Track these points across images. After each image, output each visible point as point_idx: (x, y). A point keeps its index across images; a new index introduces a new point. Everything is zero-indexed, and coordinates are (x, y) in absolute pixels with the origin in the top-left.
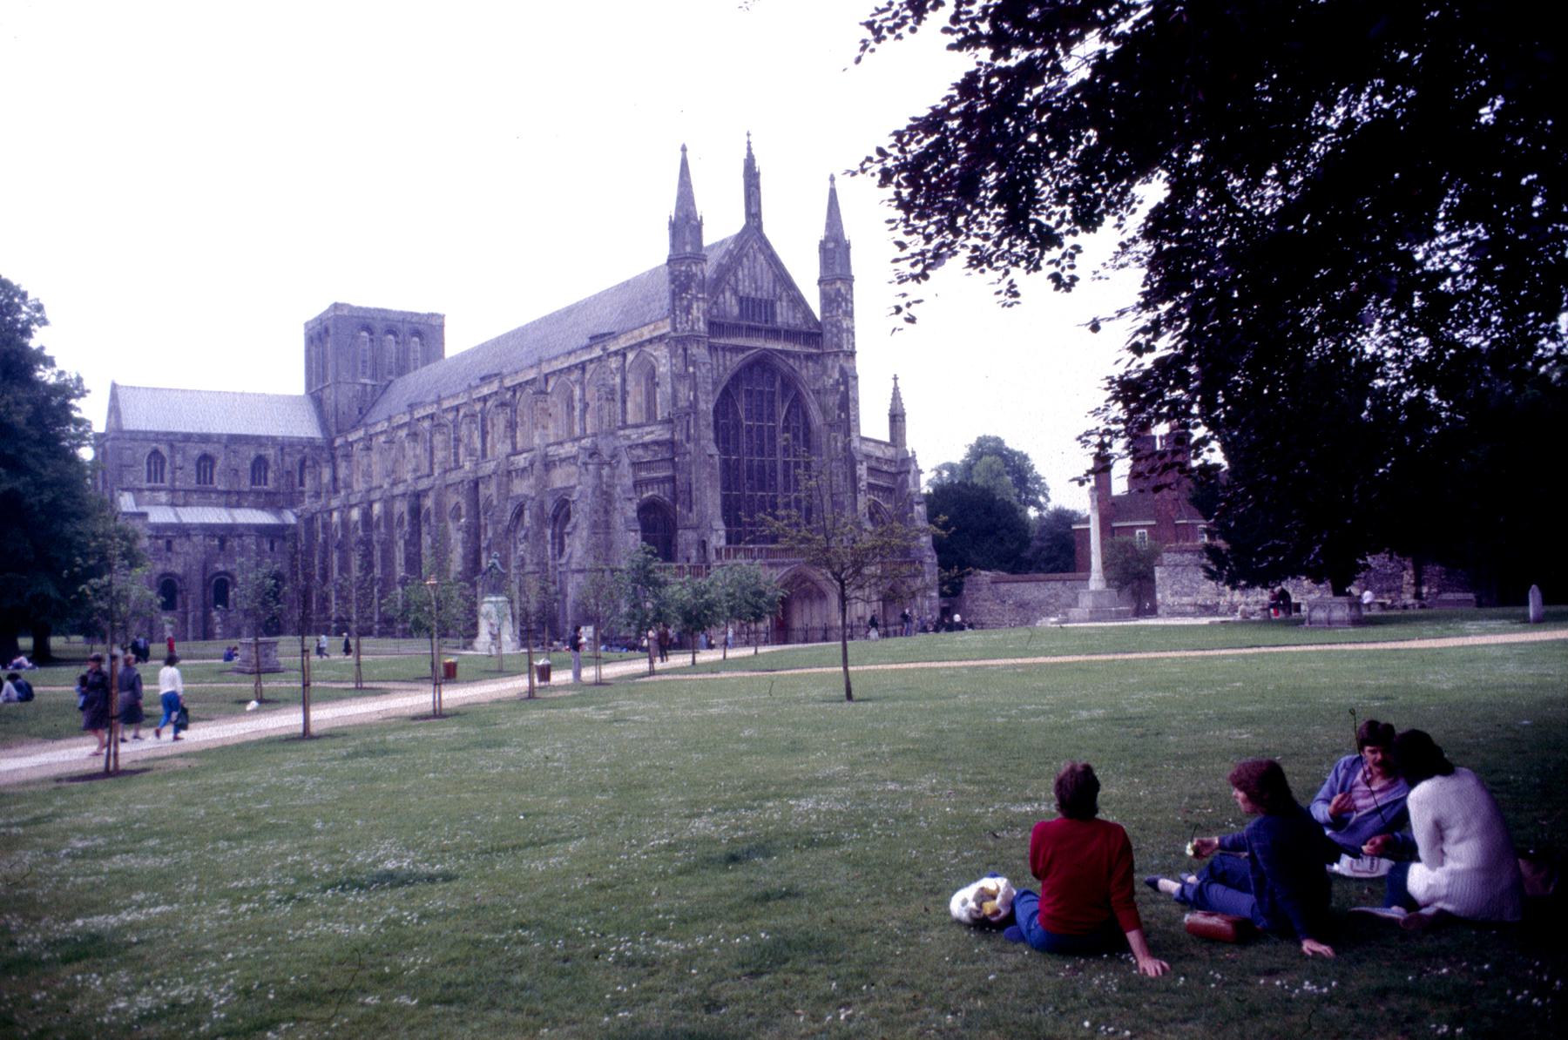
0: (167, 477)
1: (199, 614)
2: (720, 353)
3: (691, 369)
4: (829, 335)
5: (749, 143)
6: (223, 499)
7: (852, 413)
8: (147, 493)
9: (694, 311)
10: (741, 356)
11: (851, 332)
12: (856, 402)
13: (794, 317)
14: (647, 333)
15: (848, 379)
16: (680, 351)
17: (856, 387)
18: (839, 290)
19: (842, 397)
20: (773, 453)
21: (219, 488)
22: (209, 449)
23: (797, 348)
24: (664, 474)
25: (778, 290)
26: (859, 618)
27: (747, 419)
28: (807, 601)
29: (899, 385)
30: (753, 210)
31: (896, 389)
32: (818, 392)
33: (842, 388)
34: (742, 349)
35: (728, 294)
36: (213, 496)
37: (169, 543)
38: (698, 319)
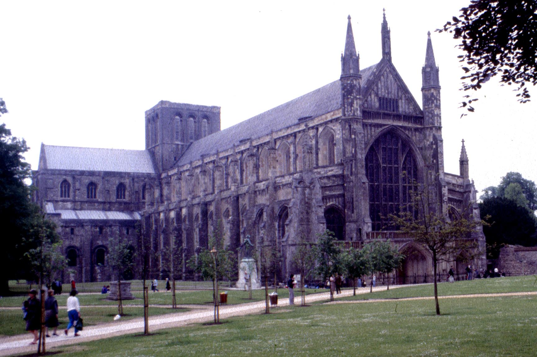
0: (71, 194)
1: (88, 268)
2: (369, 128)
3: (353, 136)
4: (427, 118)
6: (101, 206)
7: (439, 160)
8: (60, 203)
9: (355, 105)
10: (380, 129)
11: (439, 116)
12: (442, 154)
13: (409, 108)
14: (329, 117)
15: (437, 142)
16: (347, 126)
17: (442, 146)
18: (433, 94)
20: (397, 181)
21: (99, 200)
22: (94, 179)
23: (410, 125)
24: (338, 193)
25: (400, 94)
27: (383, 163)
29: (465, 145)
30: (387, 51)
31: (463, 147)
32: (422, 149)
33: (434, 146)
34: (381, 126)
35: (373, 96)
36: (96, 204)
37: (72, 230)
38: (357, 109)
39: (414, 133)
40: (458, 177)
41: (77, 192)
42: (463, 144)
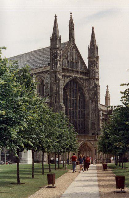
3: (57, 81)
5: (71, 16)
7: (98, 96)
9: (58, 64)
10: (69, 78)
11: (98, 73)
12: (99, 93)
14: (41, 70)
15: (97, 87)
16: (54, 76)
17: (99, 89)
18: (95, 60)
19: (95, 92)
20: (76, 107)
27: (69, 97)
28: (85, 152)
31: (107, 90)
33: (95, 89)
34: (69, 76)
39: (85, 81)
42: (107, 88)
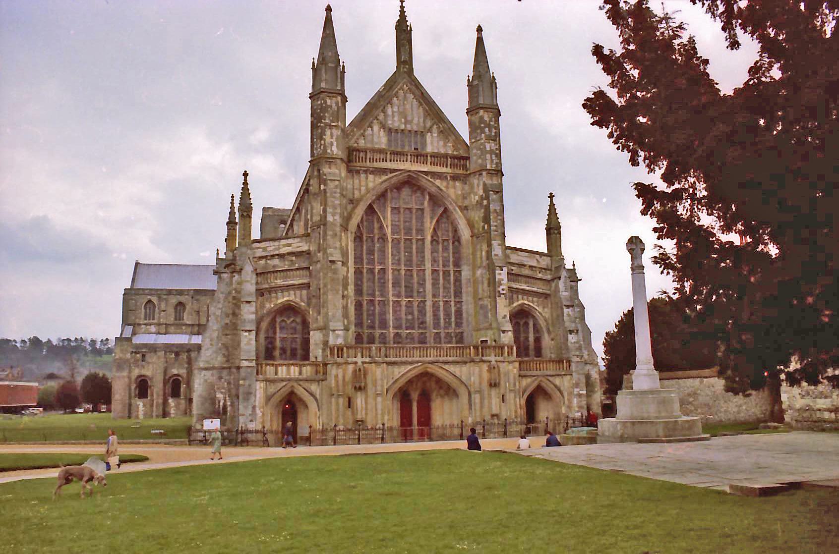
0: (156, 316)
1: (161, 401)
4: (475, 158)
6: (189, 330)
8: (143, 326)
18: (482, 118)
21: (188, 323)
22: (182, 299)
23: (444, 170)
24: (300, 282)
26: (493, 416)
32: (466, 208)
34: (384, 171)
35: (376, 128)
36: (184, 328)
37: (144, 356)
38: (332, 144)
39: (451, 183)
40: (541, 254)
41: (163, 314)
